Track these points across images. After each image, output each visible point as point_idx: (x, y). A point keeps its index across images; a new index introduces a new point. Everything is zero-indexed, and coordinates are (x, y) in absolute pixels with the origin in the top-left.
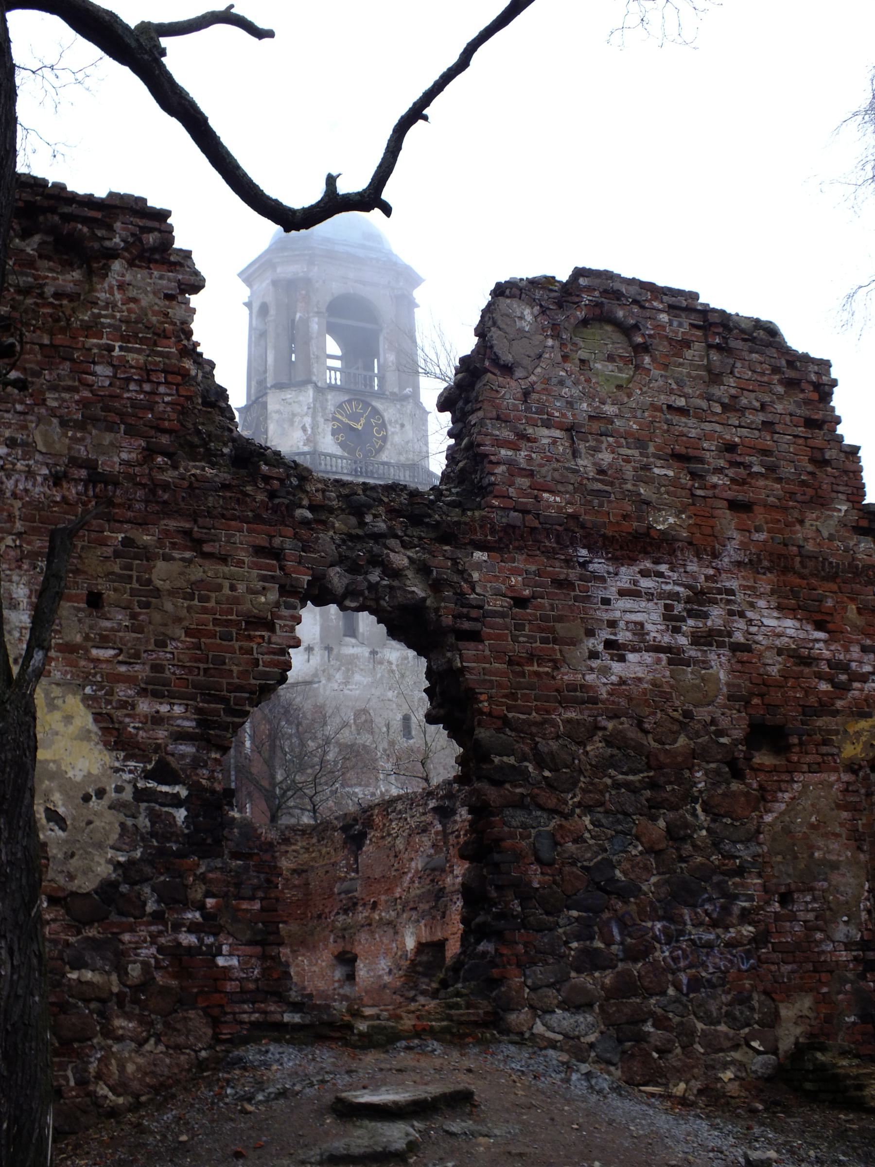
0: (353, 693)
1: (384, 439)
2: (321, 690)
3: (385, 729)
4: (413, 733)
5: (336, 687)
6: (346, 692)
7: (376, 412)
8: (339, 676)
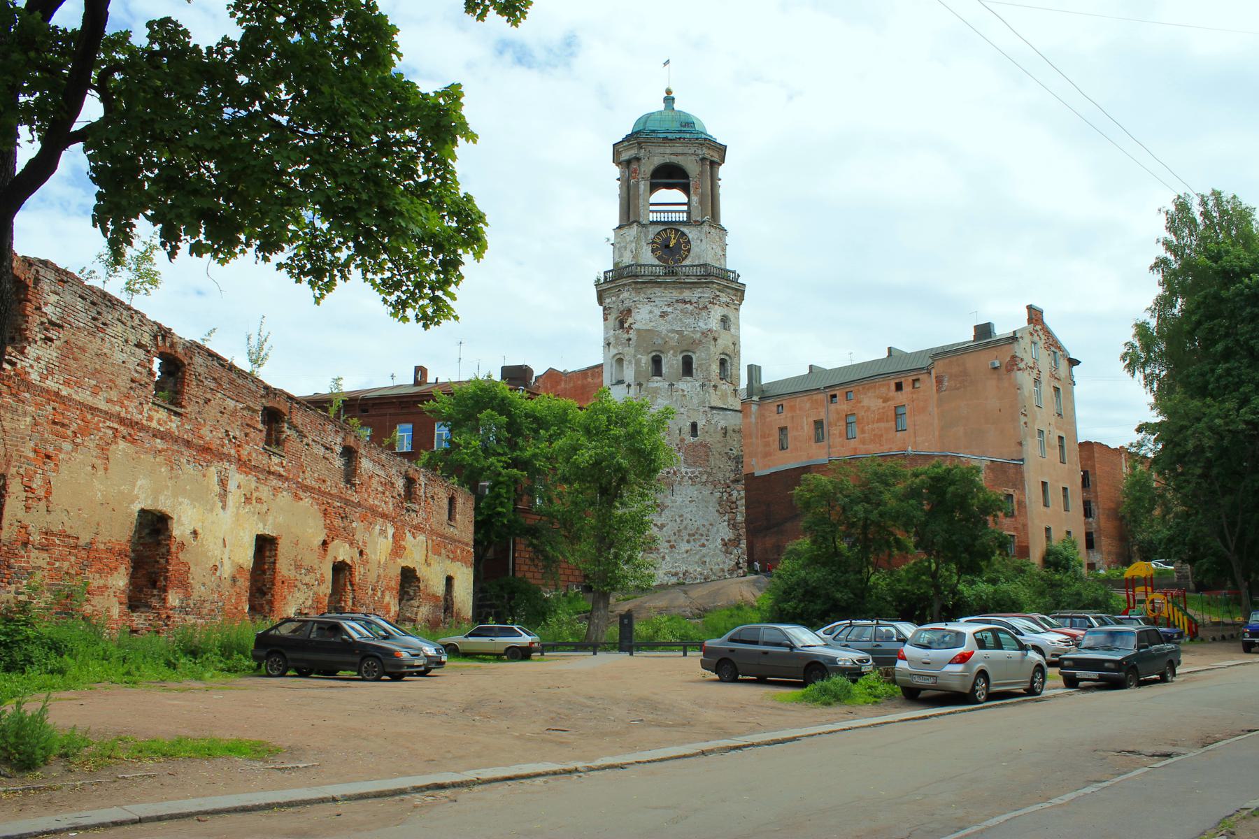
1: (689, 251)
7: (683, 234)
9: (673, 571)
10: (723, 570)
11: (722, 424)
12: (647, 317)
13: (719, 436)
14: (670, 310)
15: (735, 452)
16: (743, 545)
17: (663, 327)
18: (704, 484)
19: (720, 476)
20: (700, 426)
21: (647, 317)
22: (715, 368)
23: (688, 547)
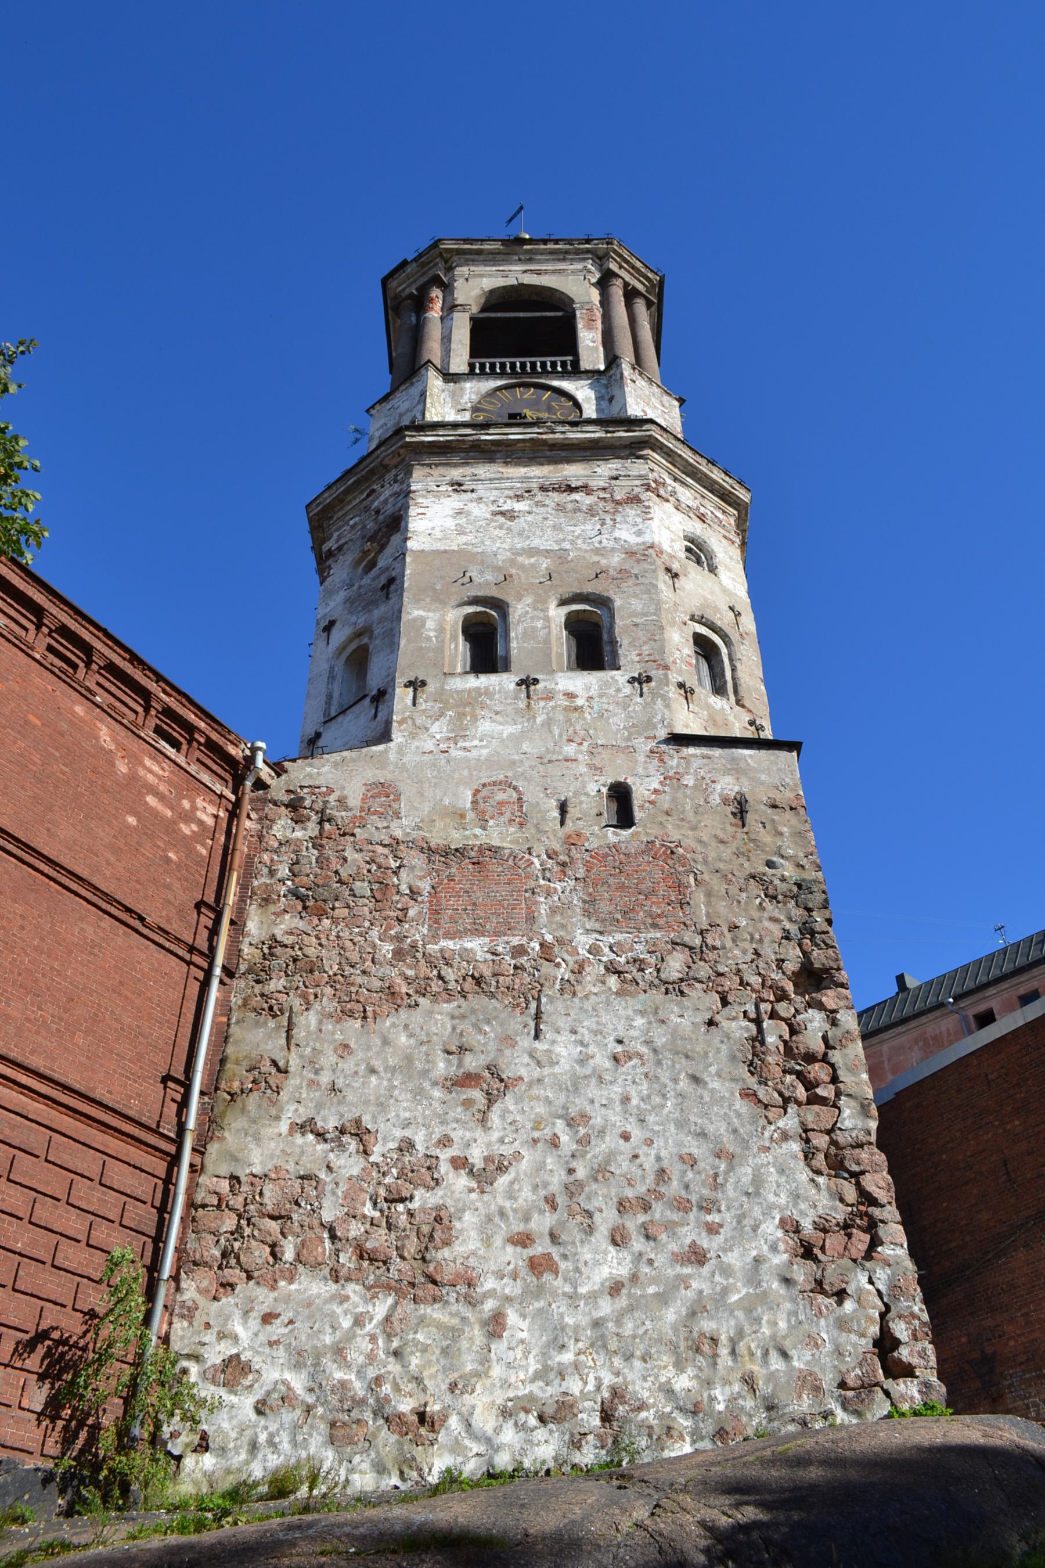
0: (474, 753)
2: (392, 756)
3: (556, 814)
4: (638, 814)
5: (429, 745)
6: (455, 753)
8: (439, 729)
9: (548, 1393)
10: (810, 1383)
11: (727, 785)
12: (451, 523)
13: (717, 823)
14: (520, 506)
15: (789, 871)
16: (895, 1247)
17: (499, 543)
18: (676, 988)
19: (738, 955)
20: (641, 792)
21: (451, 523)
22: (679, 645)
23: (613, 1265)
